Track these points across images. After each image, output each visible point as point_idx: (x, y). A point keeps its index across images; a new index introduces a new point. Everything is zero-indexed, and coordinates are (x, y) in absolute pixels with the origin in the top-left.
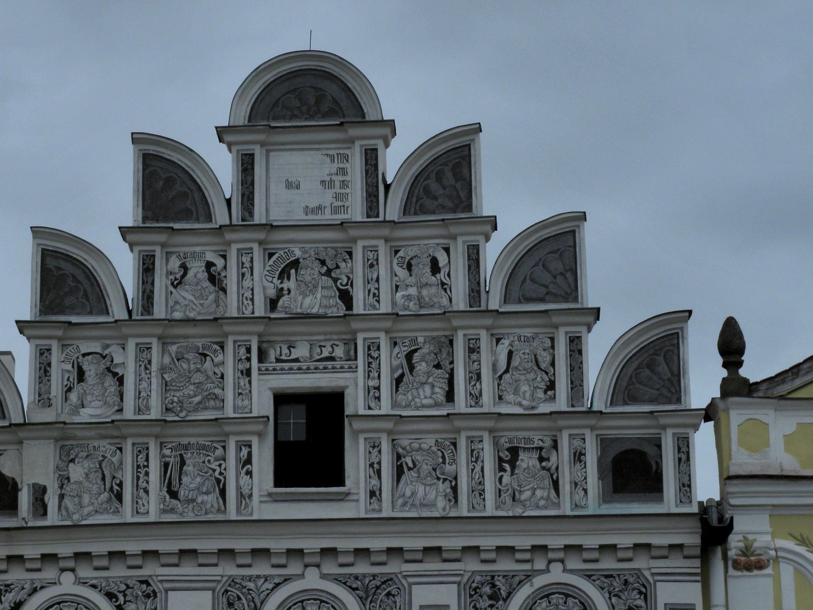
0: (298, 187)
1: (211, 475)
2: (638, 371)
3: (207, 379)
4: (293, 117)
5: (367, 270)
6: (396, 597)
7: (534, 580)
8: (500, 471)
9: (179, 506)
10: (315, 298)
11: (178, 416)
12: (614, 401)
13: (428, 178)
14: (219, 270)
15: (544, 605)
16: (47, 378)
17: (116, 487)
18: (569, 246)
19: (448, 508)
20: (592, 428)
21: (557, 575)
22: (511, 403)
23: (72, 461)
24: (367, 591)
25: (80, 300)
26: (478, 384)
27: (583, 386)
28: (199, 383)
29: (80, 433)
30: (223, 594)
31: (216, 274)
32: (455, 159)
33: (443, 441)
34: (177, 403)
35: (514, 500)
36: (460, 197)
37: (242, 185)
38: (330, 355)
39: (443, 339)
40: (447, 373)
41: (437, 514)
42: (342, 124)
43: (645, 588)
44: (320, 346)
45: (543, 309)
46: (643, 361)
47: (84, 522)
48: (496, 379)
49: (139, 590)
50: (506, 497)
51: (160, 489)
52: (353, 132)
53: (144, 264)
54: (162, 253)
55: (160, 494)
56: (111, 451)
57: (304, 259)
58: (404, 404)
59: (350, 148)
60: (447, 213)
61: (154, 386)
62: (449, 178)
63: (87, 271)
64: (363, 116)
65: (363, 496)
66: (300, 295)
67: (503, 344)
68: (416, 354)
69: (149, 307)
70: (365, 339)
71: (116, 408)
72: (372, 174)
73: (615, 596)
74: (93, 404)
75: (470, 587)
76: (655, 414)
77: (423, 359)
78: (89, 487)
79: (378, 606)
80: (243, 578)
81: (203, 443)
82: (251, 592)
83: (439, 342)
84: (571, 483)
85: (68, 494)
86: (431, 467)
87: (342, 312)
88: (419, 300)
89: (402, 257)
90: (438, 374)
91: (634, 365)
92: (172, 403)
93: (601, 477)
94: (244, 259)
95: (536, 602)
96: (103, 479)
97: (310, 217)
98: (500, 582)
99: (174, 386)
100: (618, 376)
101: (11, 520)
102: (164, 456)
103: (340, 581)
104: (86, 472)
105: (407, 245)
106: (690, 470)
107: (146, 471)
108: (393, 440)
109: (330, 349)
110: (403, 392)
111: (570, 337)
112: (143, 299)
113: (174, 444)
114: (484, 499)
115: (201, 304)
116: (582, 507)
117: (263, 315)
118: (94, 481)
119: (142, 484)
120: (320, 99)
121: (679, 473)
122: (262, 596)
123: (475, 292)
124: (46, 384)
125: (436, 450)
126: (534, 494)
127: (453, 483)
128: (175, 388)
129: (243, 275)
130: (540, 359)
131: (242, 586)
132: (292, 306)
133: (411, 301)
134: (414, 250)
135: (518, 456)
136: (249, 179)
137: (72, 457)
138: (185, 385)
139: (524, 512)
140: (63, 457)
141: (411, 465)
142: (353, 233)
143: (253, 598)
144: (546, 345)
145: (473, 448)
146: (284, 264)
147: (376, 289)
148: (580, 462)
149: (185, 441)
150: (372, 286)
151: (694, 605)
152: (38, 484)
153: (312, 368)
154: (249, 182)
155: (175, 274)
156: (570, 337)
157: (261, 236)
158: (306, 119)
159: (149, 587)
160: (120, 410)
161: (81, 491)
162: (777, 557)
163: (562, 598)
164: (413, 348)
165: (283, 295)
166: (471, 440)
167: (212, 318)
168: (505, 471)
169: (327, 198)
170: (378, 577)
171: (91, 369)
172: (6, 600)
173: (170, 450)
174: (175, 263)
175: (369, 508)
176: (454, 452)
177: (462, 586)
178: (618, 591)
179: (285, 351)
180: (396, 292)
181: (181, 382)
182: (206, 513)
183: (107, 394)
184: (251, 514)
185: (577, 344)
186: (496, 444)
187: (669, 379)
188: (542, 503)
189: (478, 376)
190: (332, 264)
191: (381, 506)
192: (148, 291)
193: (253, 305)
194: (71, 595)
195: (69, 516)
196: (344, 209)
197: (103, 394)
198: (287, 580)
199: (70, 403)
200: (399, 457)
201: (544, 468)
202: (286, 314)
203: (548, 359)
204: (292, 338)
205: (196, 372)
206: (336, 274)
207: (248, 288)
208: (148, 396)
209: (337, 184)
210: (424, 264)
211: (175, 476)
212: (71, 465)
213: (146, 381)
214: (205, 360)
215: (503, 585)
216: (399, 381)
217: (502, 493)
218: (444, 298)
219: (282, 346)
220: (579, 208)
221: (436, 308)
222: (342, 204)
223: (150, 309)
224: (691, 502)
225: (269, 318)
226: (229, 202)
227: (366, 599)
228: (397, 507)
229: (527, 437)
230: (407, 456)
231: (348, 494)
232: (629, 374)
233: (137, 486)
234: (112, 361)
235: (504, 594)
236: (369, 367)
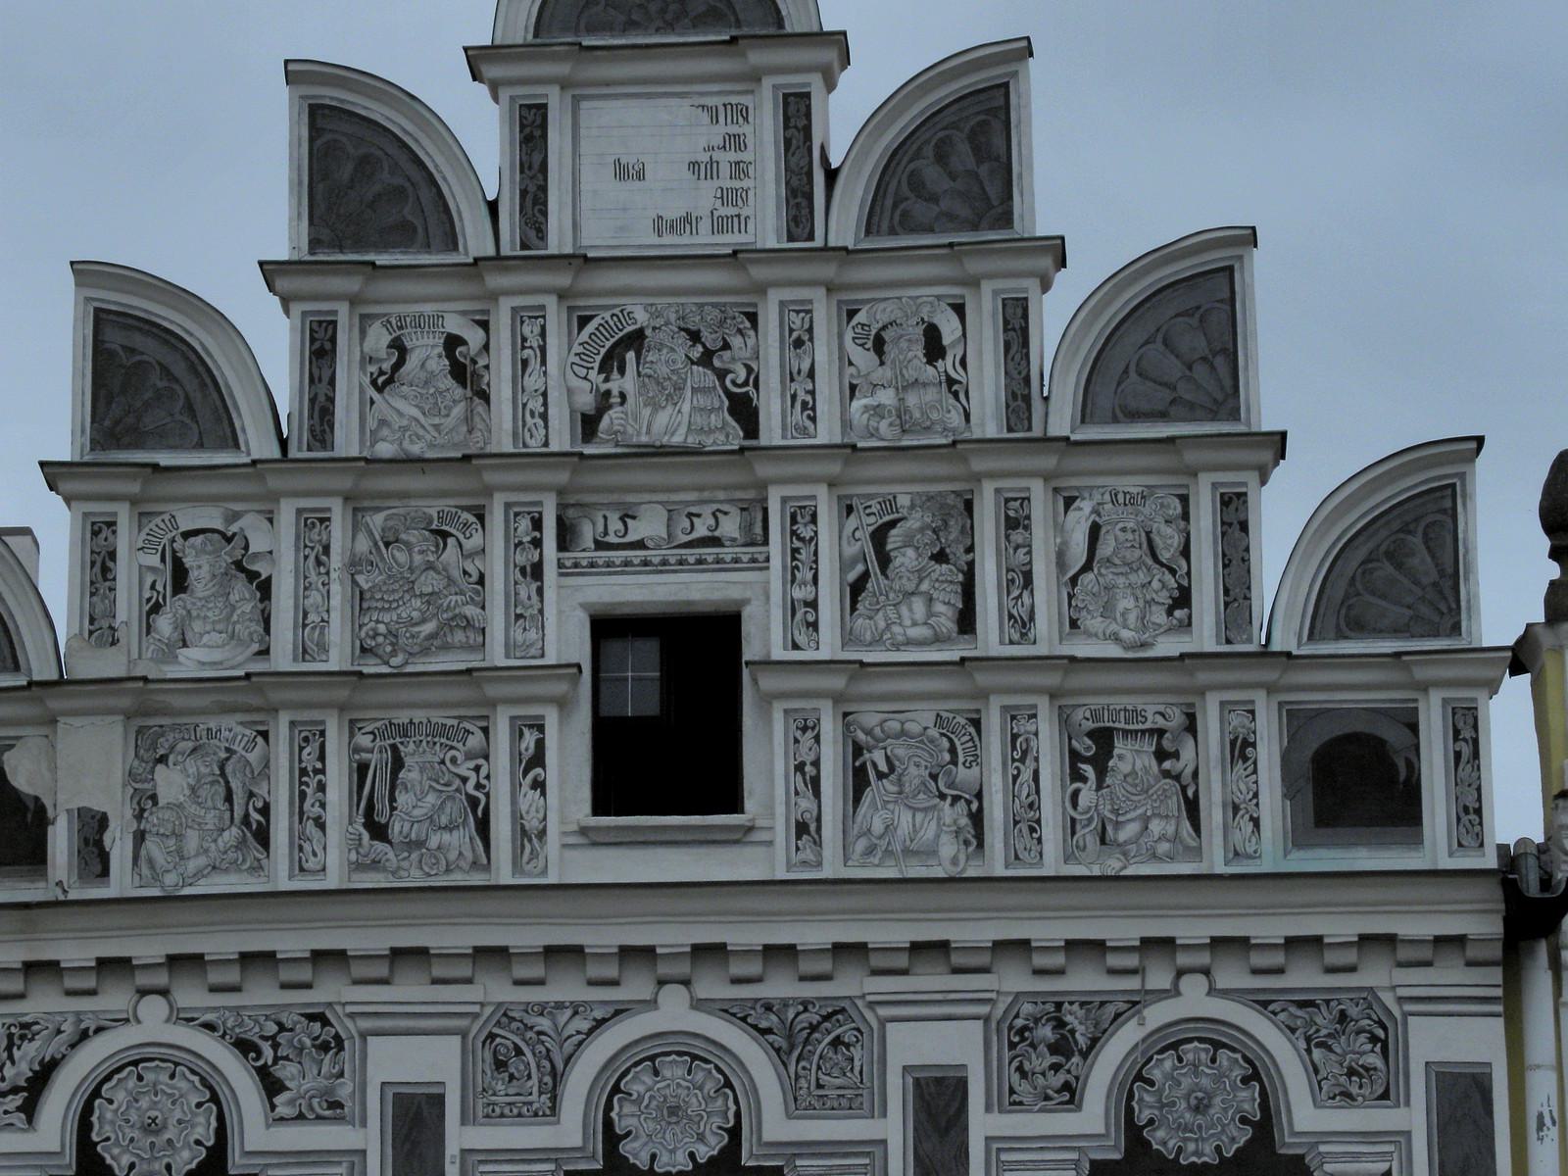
0: (641, 176)
1: (458, 790)
2: (1370, 566)
3: (449, 585)
4: (630, 25)
6: (852, 1049)
7: (1146, 1012)
8: (1073, 780)
9: (391, 855)
10: (679, 411)
11: (387, 663)
12: (1316, 631)
13: (917, 156)
14: (472, 353)
15: (1168, 1065)
16: (108, 584)
17: (255, 816)
18: (1221, 301)
19: (962, 857)
20: (1271, 689)
21: (1194, 1000)
22: (1096, 635)
23: (162, 760)
24: (790, 1036)
25: (178, 417)
26: (1026, 594)
27: (1250, 599)
28: (432, 594)
29: (178, 701)
30: (484, 1043)
31: (468, 362)
32: (978, 113)
33: (951, 716)
34: (385, 637)
35: (1103, 842)
36: (988, 198)
37: (522, 172)
38: (710, 534)
39: (951, 500)
40: (958, 570)
41: (939, 873)
42: (734, 40)
43: (1385, 1029)
44: (690, 515)
45: (1164, 435)
46: (1379, 546)
47: (187, 891)
48: (1066, 584)
49: (306, 1034)
50: (1088, 836)
51: (350, 820)
52: (757, 57)
53: (313, 340)
54: (350, 319)
55: (351, 829)
56: (246, 739)
57: (654, 329)
58: (868, 637)
59: (752, 92)
60: (960, 230)
61: (336, 601)
62: (963, 155)
63: (193, 357)
64: (780, 23)
65: (781, 832)
66: (645, 405)
67: (1080, 509)
68: (894, 532)
69: (324, 431)
70: (784, 500)
71: (255, 647)
72: (798, 147)
73: (1319, 1045)
74: (206, 639)
75: (1010, 1028)
76: (1405, 658)
78: (200, 817)
79: (814, 1067)
80: (527, 1007)
81: (441, 721)
82: (543, 1038)
83: (942, 506)
84: (1224, 806)
85: (154, 830)
86: (927, 772)
87: (736, 442)
88: (899, 417)
89: (863, 325)
90: (942, 575)
91: (1361, 553)
92: (374, 638)
93: (1290, 792)
94: (527, 330)
95: (1150, 1059)
96: (229, 798)
97: (668, 239)
98: (1073, 1018)
99: (378, 600)
100: (1326, 578)
101: (32, 886)
102: (357, 750)
103: (734, 1015)
104: (193, 783)
105: (874, 300)
106: (1479, 778)
107: (320, 781)
108: (846, 715)
109: (712, 522)
110: (867, 613)
111: (1222, 495)
112: (311, 417)
113: (378, 724)
114: (1039, 840)
115: (436, 427)
116: (1249, 857)
117: (567, 448)
118: (210, 803)
121: (1456, 784)
122: (568, 1047)
123: (1020, 397)
124: (105, 597)
125: (937, 735)
126: (1147, 828)
127: (975, 806)
128: (379, 605)
129: (525, 363)
130: (1157, 540)
131: (526, 1025)
132: (630, 430)
133: (883, 418)
134: (888, 310)
135: (1112, 747)
136: (537, 158)
137: (161, 752)
138: (402, 598)
139: (1125, 867)
140: (142, 751)
141: (883, 767)
142: (759, 273)
143: (548, 1050)
144: (1171, 512)
145: (1015, 731)
146: (612, 341)
147: (808, 392)
148: (1244, 763)
149: (402, 717)
150: (800, 387)
151: (1489, 1065)
152: (91, 810)
153: (672, 560)
154: (536, 166)
155: (381, 360)
156: (1222, 495)
157: (563, 280)
158: (657, 30)
159: (327, 1028)
160: (265, 652)
161: (181, 824)
163: (1207, 1051)
164: (887, 518)
165: (610, 407)
166: (1011, 714)
167: (460, 455)
168: (1084, 780)
169: (703, 199)
170: (814, 1006)
171: (201, 566)
172: (22, 1058)
173: (371, 737)
174: (379, 339)
175: (794, 859)
176: (976, 739)
177: (994, 1025)
178: (1325, 1036)
179: (615, 525)
180: (851, 399)
181: (394, 591)
182: (448, 871)
183: (235, 618)
184: (544, 872)
185: (1237, 510)
186: (1064, 721)
187: (1435, 584)
188: (1164, 847)
189: (1024, 577)
190: (714, 340)
191: (821, 855)
192: (322, 398)
193: (546, 427)
194: (160, 1045)
195: (156, 878)
196: (740, 222)
198: (620, 1012)
199: (158, 637)
200: (858, 750)
201: (1166, 774)
202: (617, 445)
203: (1176, 541)
204: (630, 498)
205: (427, 569)
206: (723, 361)
207: (536, 391)
208: (323, 621)
209: (725, 170)
210: (910, 340)
211: (382, 791)
212: (160, 768)
213: (318, 590)
214: (445, 545)
215: (1081, 1023)
216: (857, 588)
217: (1078, 827)
218: (953, 412)
219: (608, 514)
220: (1238, 217)
221: (937, 432)
222: (732, 211)
223: (328, 437)
224: (1482, 845)
225: (581, 455)
226: (493, 207)
228: (856, 856)
229: (1130, 707)
230: (875, 747)
231: (750, 829)
233: (301, 813)
234: (246, 548)
235: (1082, 1042)
236: (794, 559)
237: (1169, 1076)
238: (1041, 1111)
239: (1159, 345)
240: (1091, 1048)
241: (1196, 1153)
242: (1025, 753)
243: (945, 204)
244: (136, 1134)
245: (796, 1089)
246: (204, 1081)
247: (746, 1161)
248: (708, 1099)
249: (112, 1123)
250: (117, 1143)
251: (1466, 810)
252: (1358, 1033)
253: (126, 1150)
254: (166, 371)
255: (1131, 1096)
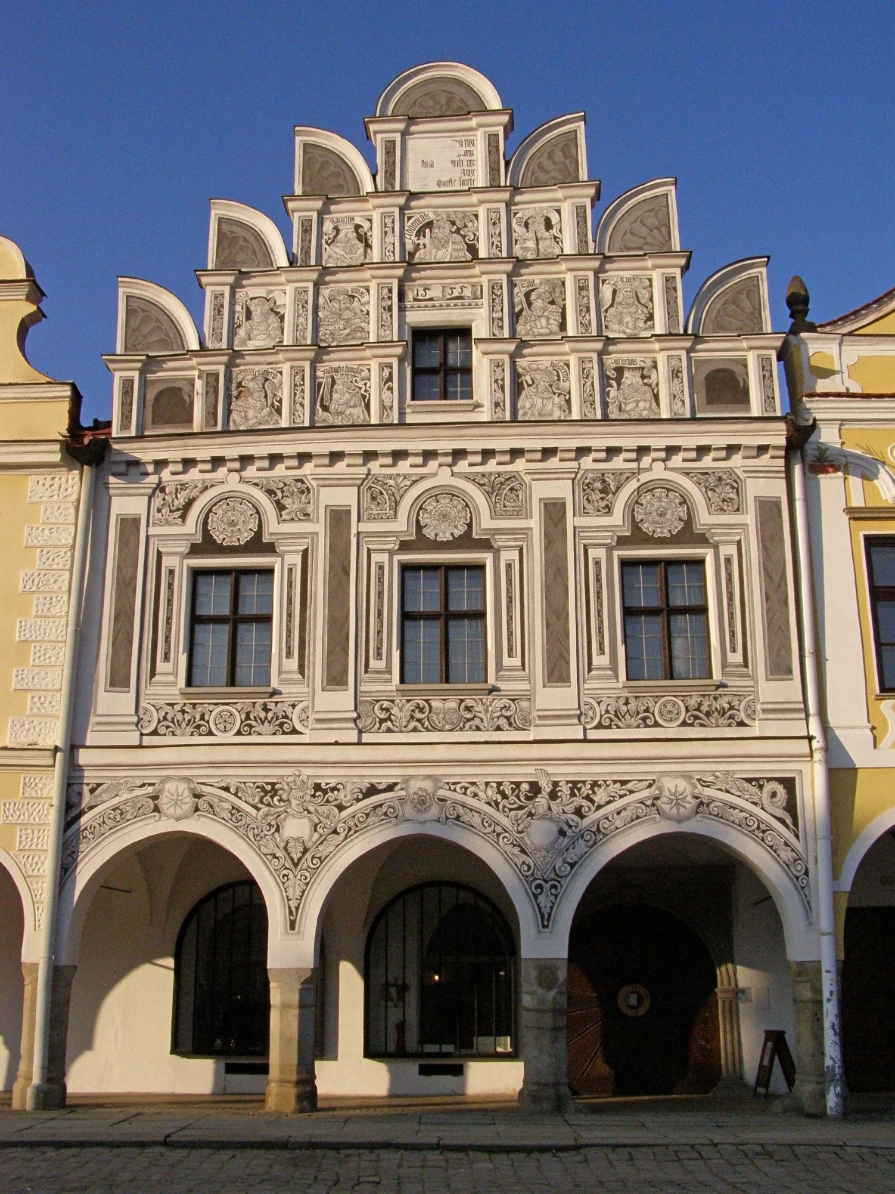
0: (432, 166)
5: (491, 227)
15: (648, 498)
17: (276, 403)
24: (493, 487)
35: (620, 410)
39: (556, 281)
53: (303, 226)
59: (475, 135)
62: (559, 156)
70: (489, 281)
71: (278, 340)
73: (710, 490)
77: (539, 297)
91: (722, 301)
94: (387, 221)
96: (266, 397)
98: (609, 479)
115: (351, 258)
119: (298, 399)
120: (450, 100)
122: (401, 492)
127: (567, 397)
129: (386, 233)
130: (640, 295)
137: (240, 380)
141: (530, 382)
149: (335, 365)
160: (282, 342)
162: (847, 463)
166: (582, 361)
168: (612, 387)
169: (457, 173)
171: (257, 311)
179: (421, 292)
187: (752, 313)
197: (267, 329)
201: (646, 384)
203: (647, 295)
209: (465, 163)
222: (467, 178)
227: (492, 493)
232: (717, 309)
233: (294, 401)
234: (275, 303)
235: (613, 489)
237: (649, 502)
238: (597, 516)
239: (639, 223)
240: (617, 491)
241: (661, 533)
242: (588, 375)
243: (552, 174)
244: (226, 526)
245: (495, 507)
246: (253, 506)
247: (474, 536)
248: (459, 512)
249: (216, 522)
250: (218, 530)
251: (768, 397)
252: (727, 485)
253: (221, 533)
254: (245, 240)
255: (633, 510)
